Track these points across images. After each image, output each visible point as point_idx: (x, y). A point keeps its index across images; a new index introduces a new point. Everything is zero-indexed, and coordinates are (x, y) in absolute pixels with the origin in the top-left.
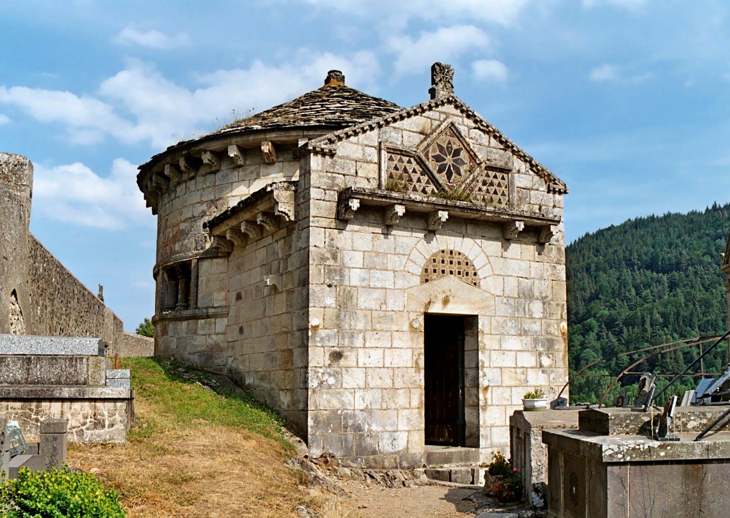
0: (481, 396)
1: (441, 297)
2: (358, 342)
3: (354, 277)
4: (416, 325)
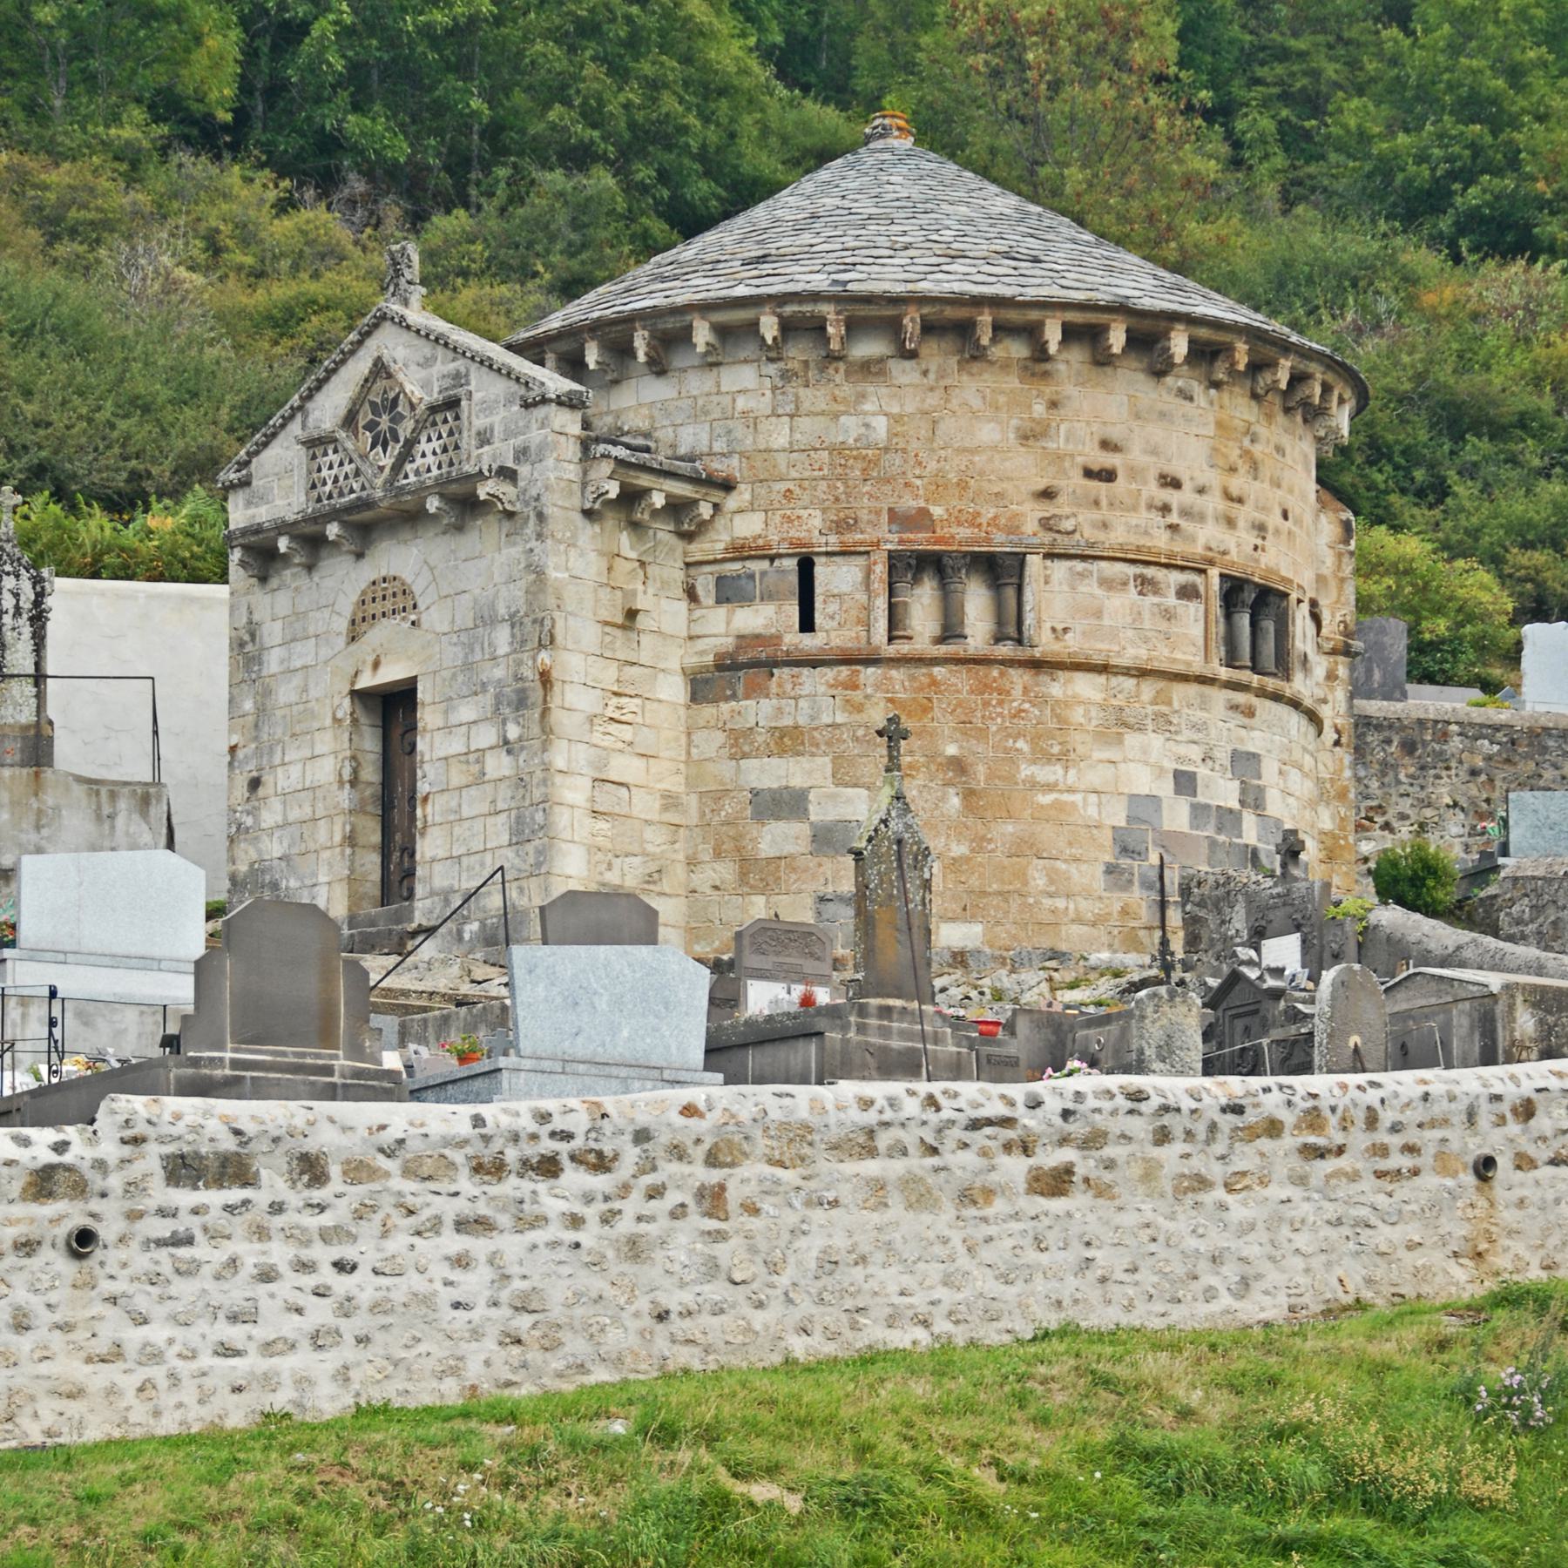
0: (419, 812)
1: (370, 659)
2: (277, 760)
3: (273, 662)
4: (340, 715)
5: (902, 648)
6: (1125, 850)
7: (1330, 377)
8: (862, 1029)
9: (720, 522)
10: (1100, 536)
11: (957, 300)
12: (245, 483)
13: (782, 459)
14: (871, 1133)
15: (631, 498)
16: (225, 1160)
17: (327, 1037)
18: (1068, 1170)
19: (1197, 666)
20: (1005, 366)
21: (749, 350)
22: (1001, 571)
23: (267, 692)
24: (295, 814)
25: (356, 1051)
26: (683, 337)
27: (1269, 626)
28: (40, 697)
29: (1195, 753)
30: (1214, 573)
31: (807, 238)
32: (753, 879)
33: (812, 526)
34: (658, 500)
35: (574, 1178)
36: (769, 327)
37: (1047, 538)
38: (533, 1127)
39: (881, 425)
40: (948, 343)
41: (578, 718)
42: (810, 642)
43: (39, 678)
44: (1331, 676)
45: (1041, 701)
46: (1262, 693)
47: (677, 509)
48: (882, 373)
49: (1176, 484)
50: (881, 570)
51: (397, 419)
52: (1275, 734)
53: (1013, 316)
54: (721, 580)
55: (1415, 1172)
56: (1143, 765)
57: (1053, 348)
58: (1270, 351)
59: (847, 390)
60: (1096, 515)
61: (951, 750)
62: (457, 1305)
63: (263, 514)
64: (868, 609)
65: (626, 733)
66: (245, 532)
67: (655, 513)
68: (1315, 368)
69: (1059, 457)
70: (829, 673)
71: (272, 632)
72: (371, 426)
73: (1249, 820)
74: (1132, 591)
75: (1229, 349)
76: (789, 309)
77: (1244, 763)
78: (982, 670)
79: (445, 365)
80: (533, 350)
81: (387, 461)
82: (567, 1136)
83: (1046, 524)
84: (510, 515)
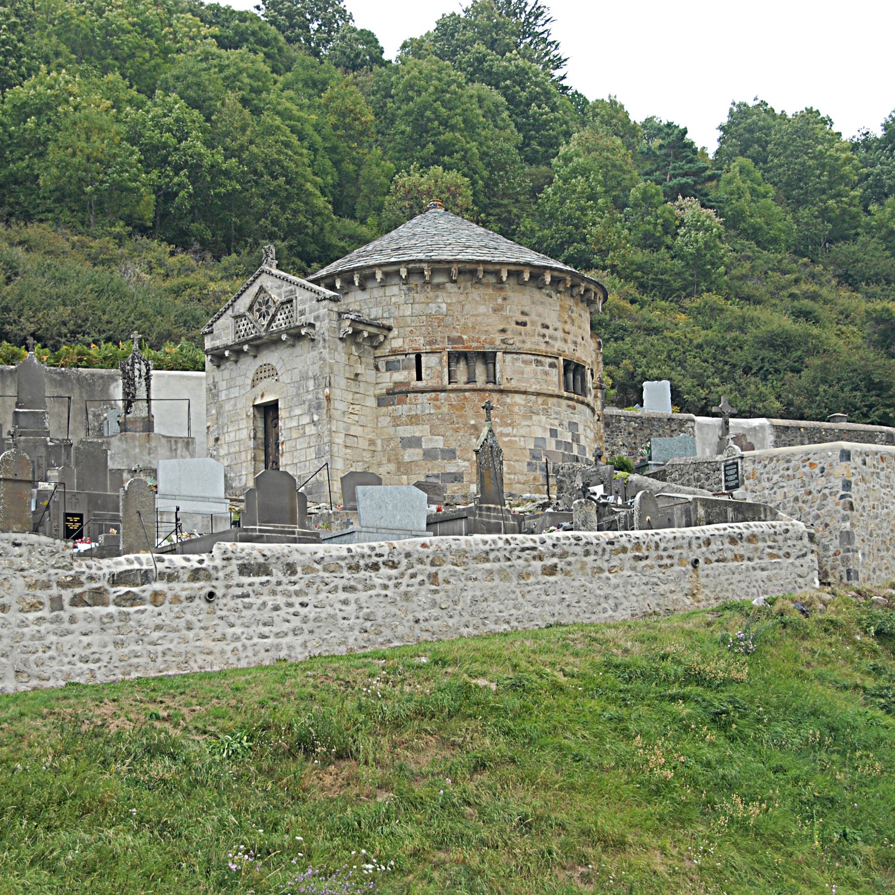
3: (223, 396)
5: (454, 386)
6: (534, 457)
7: (597, 290)
8: (481, 515)
9: (387, 342)
10: (521, 345)
11: (471, 262)
12: (211, 332)
13: (409, 319)
14: (487, 553)
15: (356, 333)
16: (260, 565)
17: (293, 521)
18: (555, 566)
19: (557, 392)
20: (487, 285)
21: (396, 280)
22: (488, 358)
23: (221, 407)
24: (232, 450)
25: (303, 526)
26: (373, 276)
27: (579, 378)
28: (149, 407)
29: (556, 422)
30: (561, 358)
31: (413, 242)
32: (402, 469)
33: (420, 343)
34: (366, 334)
35: (384, 570)
36: (404, 273)
37: (504, 346)
38: (369, 552)
39: (444, 306)
40: (468, 277)
41: (339, 412)
42: (420, 384)
43: (148, 400)
44: (596, 397)
45: (504, 404)
46: (578, 401)
47: (372, 337)
48: (444, 288)
49: (547, 327)
50: (445, 358)
51: (268, 307)
52: (582, 416)
53: (490, 268)
54: (387, 363)
55: (672, 565)
56: (539, 426)
57: (504, 279)
58: (577, 280)
59: (431, 294)
60: (521, 338)
61: (472, 422)
62: (344, 618)
63: (218, 343)
64: (442, 372)
65: (356, 418)
66: (212, 349)
67: (364, 339)
68: (592, 287)
69: (507, 318)
70: (428, 395)
71: (223, 385)
72: (259, 310)
73: (575, 446)
74: (534, 365)
75: (564, 280)
76: (411, 266)
77: (573, 426)
78: (482, 394)
79: (287, 287)
80: (316, 282)
81: (265, 323)
82: (381, 555)
83: (503, 341)
84: (313, 340)
